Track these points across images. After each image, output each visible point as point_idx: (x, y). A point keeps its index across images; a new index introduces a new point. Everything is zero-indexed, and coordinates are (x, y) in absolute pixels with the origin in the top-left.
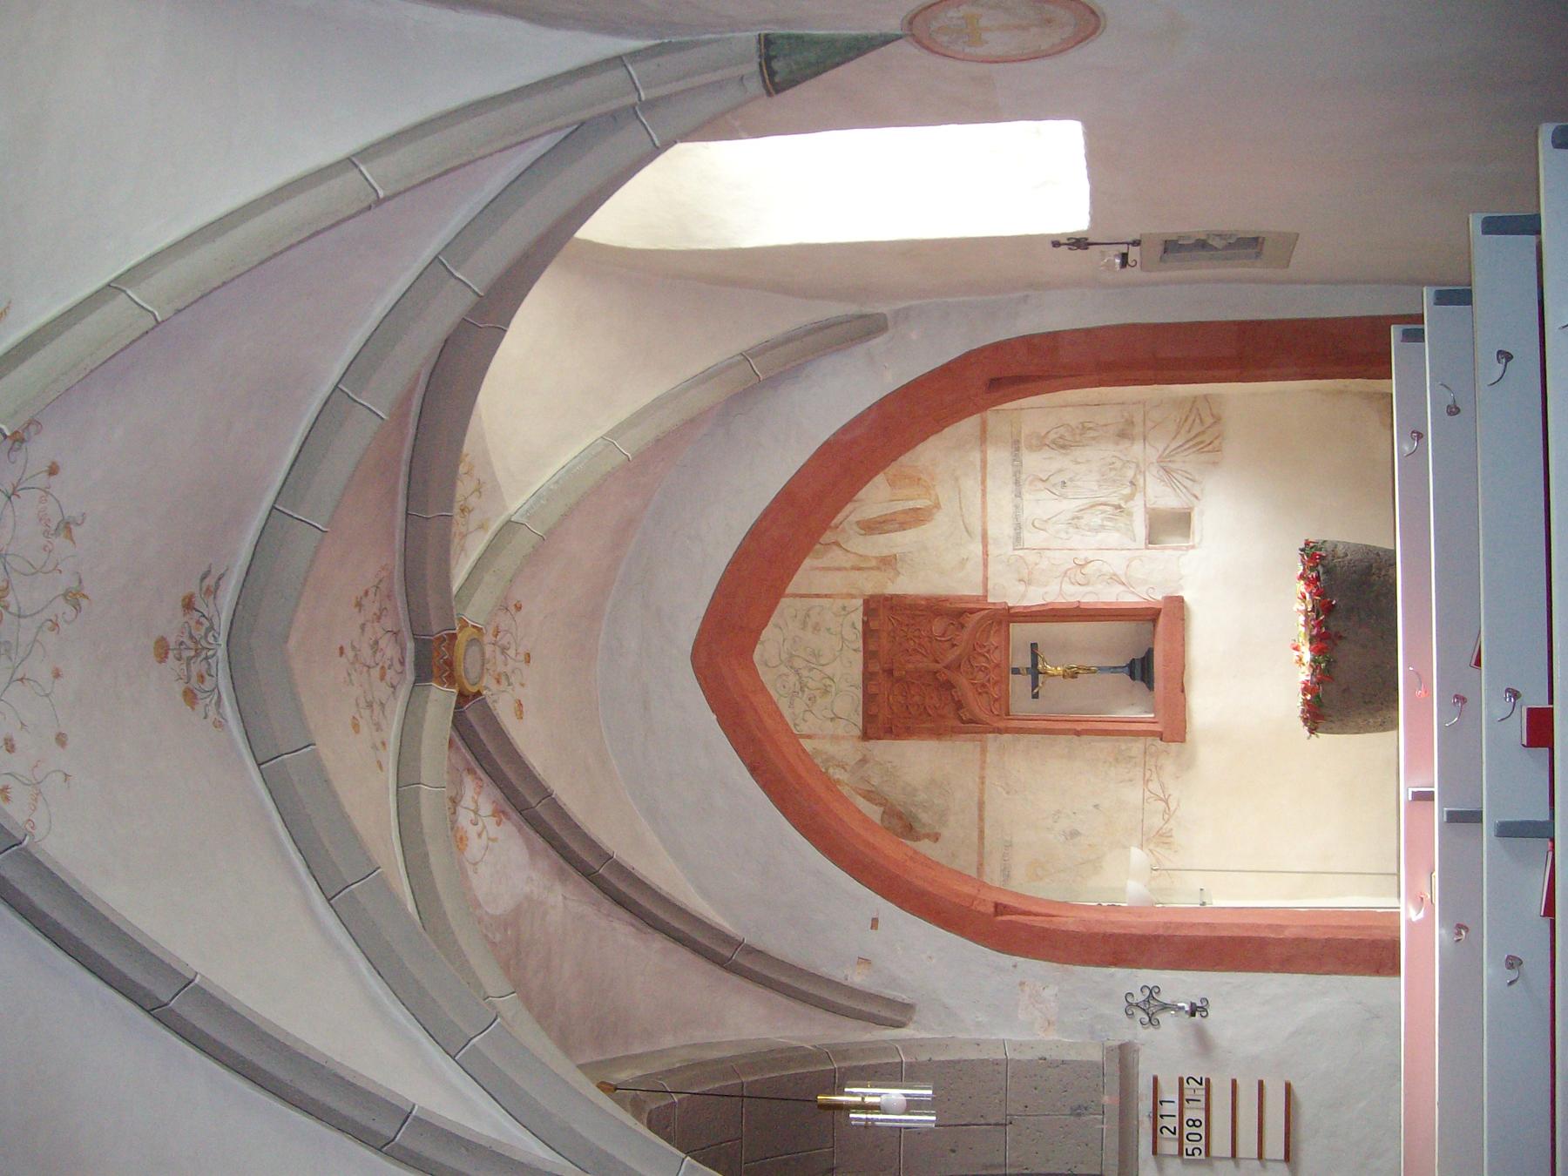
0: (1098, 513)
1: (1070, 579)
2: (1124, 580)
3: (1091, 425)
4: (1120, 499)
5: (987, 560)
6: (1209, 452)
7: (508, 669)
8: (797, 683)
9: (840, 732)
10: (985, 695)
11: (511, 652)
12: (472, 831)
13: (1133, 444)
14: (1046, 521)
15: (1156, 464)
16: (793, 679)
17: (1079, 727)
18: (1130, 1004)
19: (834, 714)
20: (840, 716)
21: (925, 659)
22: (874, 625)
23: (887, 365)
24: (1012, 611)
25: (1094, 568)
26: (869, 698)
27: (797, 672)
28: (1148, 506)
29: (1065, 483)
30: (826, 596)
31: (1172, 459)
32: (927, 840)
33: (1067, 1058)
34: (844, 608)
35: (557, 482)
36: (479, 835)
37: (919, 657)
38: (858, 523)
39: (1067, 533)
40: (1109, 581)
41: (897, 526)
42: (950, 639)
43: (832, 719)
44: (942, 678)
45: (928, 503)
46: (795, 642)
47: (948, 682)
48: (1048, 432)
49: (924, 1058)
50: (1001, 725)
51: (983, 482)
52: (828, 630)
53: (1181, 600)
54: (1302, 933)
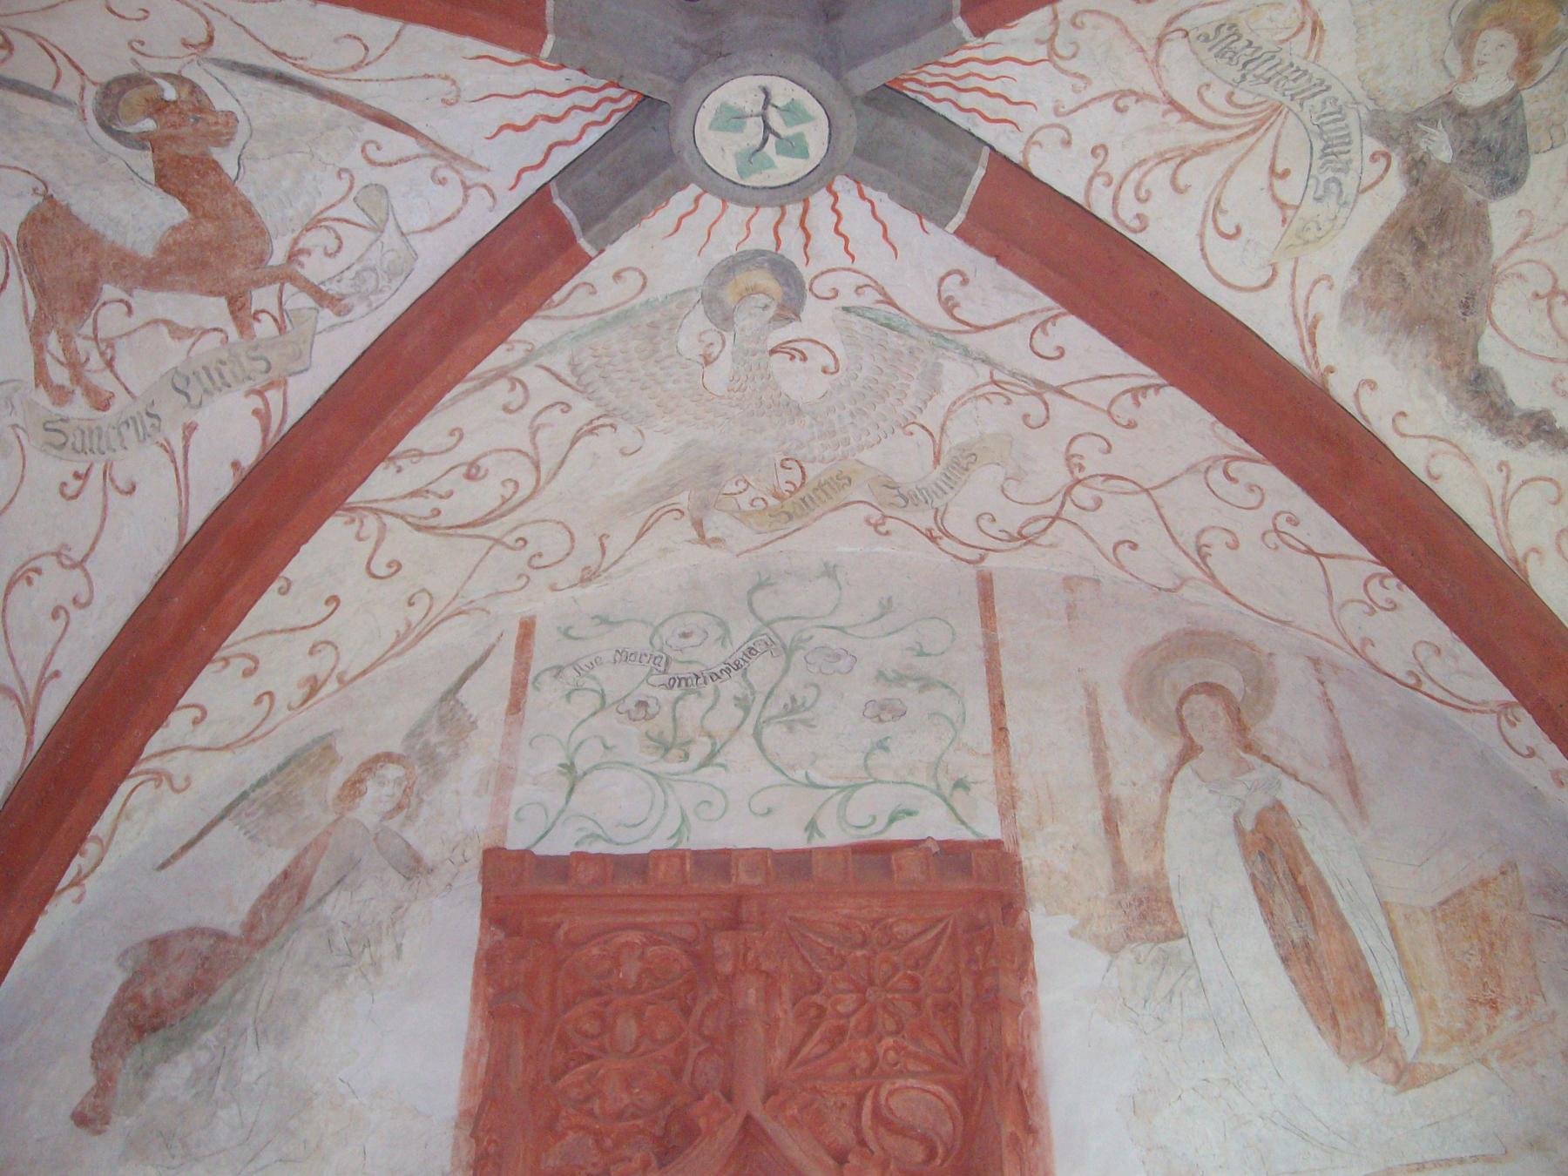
8: (695, 668)
9: (520, 793)
16: (712, 657)
19: (585, 774)
20: (578, 789)
21: (780, 1054)
30: (1000, 731)
32: (90, 1081)
34: (960, 784)
38: (1279, 807)
41: (1296, 936)
42: (862, 1143)
43: (569, 767)
46: (838, 657)
47: (691, 1133)
52: (882, 746)
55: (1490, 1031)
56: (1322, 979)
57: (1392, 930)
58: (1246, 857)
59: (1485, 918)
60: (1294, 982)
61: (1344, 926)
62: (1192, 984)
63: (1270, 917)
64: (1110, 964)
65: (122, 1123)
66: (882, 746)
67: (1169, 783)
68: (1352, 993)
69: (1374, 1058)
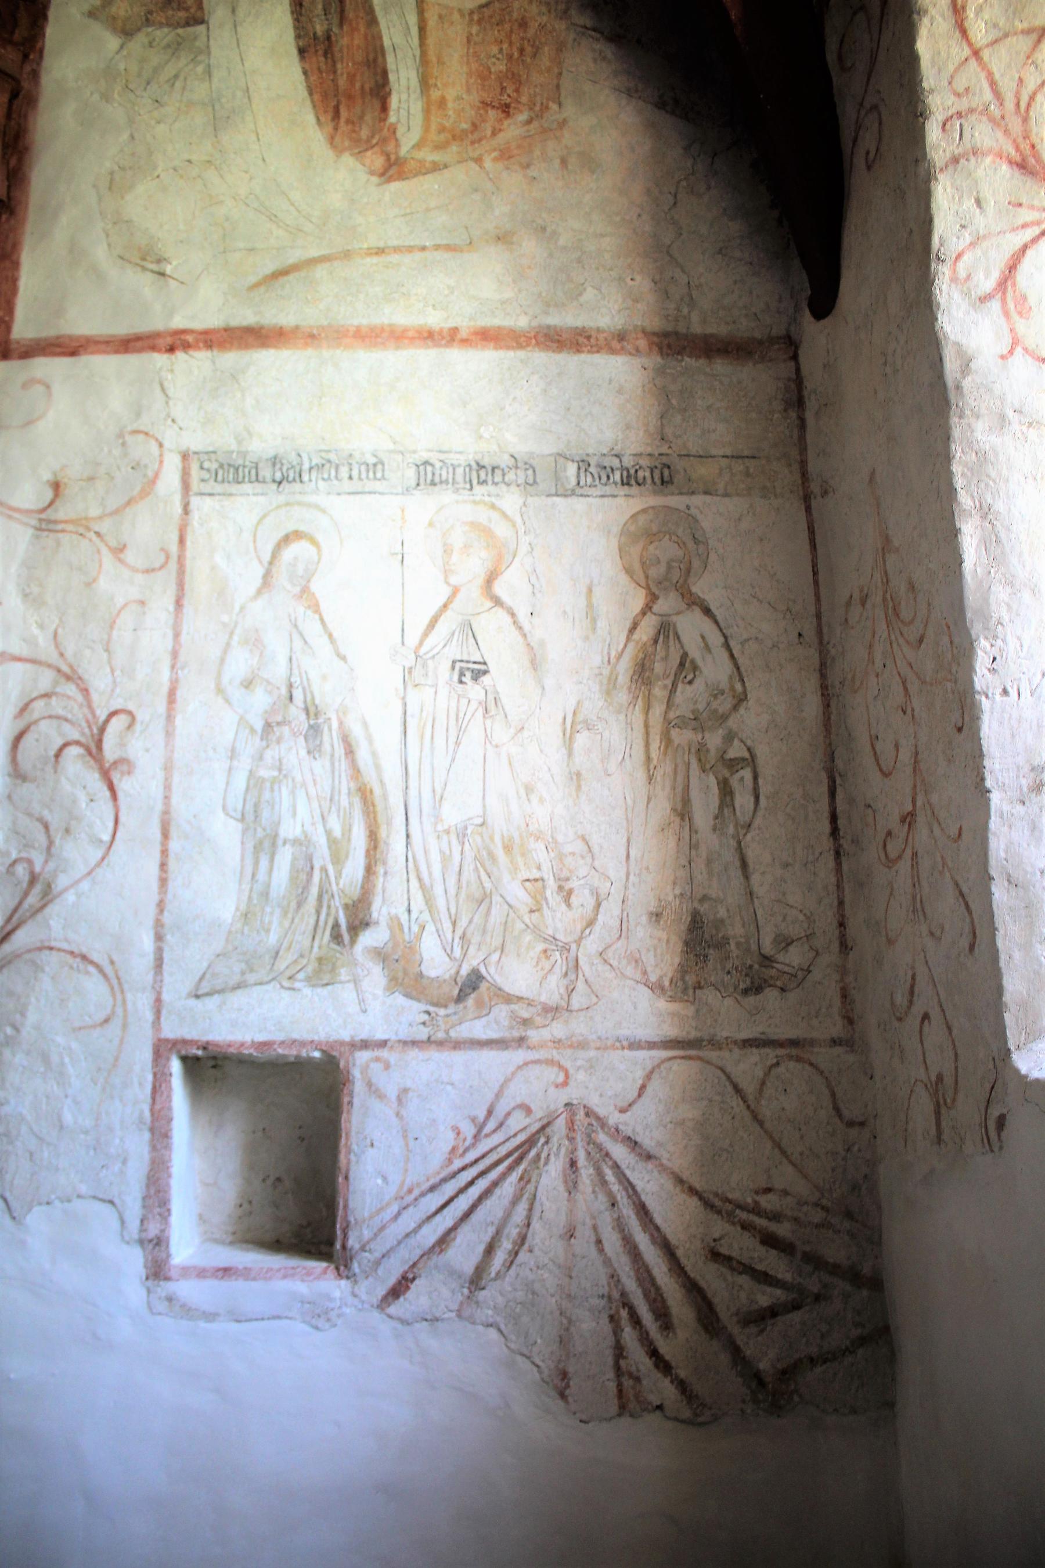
0: (335, 825)
1: (46, 695)
3: (743, 800)
4: (395, 924)
5: (154, 348)
6: (619, 1351)
13: (657, 988)
14: (305, 590)
15: (563, 1096)
25: (82, 799)
28: (363, 1057)
29: (478, 675)
31: (586, 1172)
39: (248, 684)
40: (21, 870)
41: (319, 29)
45: (408, 139)
48: (707, 611)
55: (494, 134)
56: (335, 72)
57: (422, 29)
59: (523, 24)
60: (305, 73)
61: (372, 21)
62: (200, 69)
63: (298, 8)
64: (122, 47)
68: (362, 88)
69: (366, 150)
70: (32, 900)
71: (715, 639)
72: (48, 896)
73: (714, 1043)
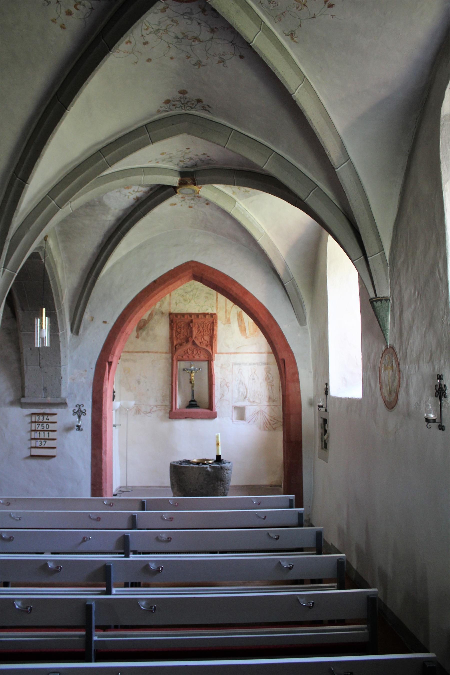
2: (222, 399)
3: (273, 388)
4: (249, 398)
6: (264, 426)
7: (186, 201)
9: (172, 306)
10: (184, 353)
11: (192, 202)
12: (131, 190)
16: (189, 290)
17: (174, 384)
18: (80, 406)
21: (196, 334)
22: (207, 317)
23: (290, 326)
24: (212, 362)
26: (183, 315)
27: (192, 291)
30: (217, 300)
31: (262, 415)
32: (136, 334)
33: (62, 386)
35: (249, 217)
36: (130, 193)
37: (197, 332)
39: (238, 380)
43: (176, 303)
44: (190, 339)
48: (271, 374)
49: (61, 339)
50: (175, 359)
51: (255, 353)
53: (216, 417)
54: (104, 461)
58: (237, 316)
61: (245, 324)
65: (140, 338)
66: (206, 301)
67: (232, 308)
70: (223, 396)
71: (271, 376)
72: (224, 396)
73: (271, 406)
